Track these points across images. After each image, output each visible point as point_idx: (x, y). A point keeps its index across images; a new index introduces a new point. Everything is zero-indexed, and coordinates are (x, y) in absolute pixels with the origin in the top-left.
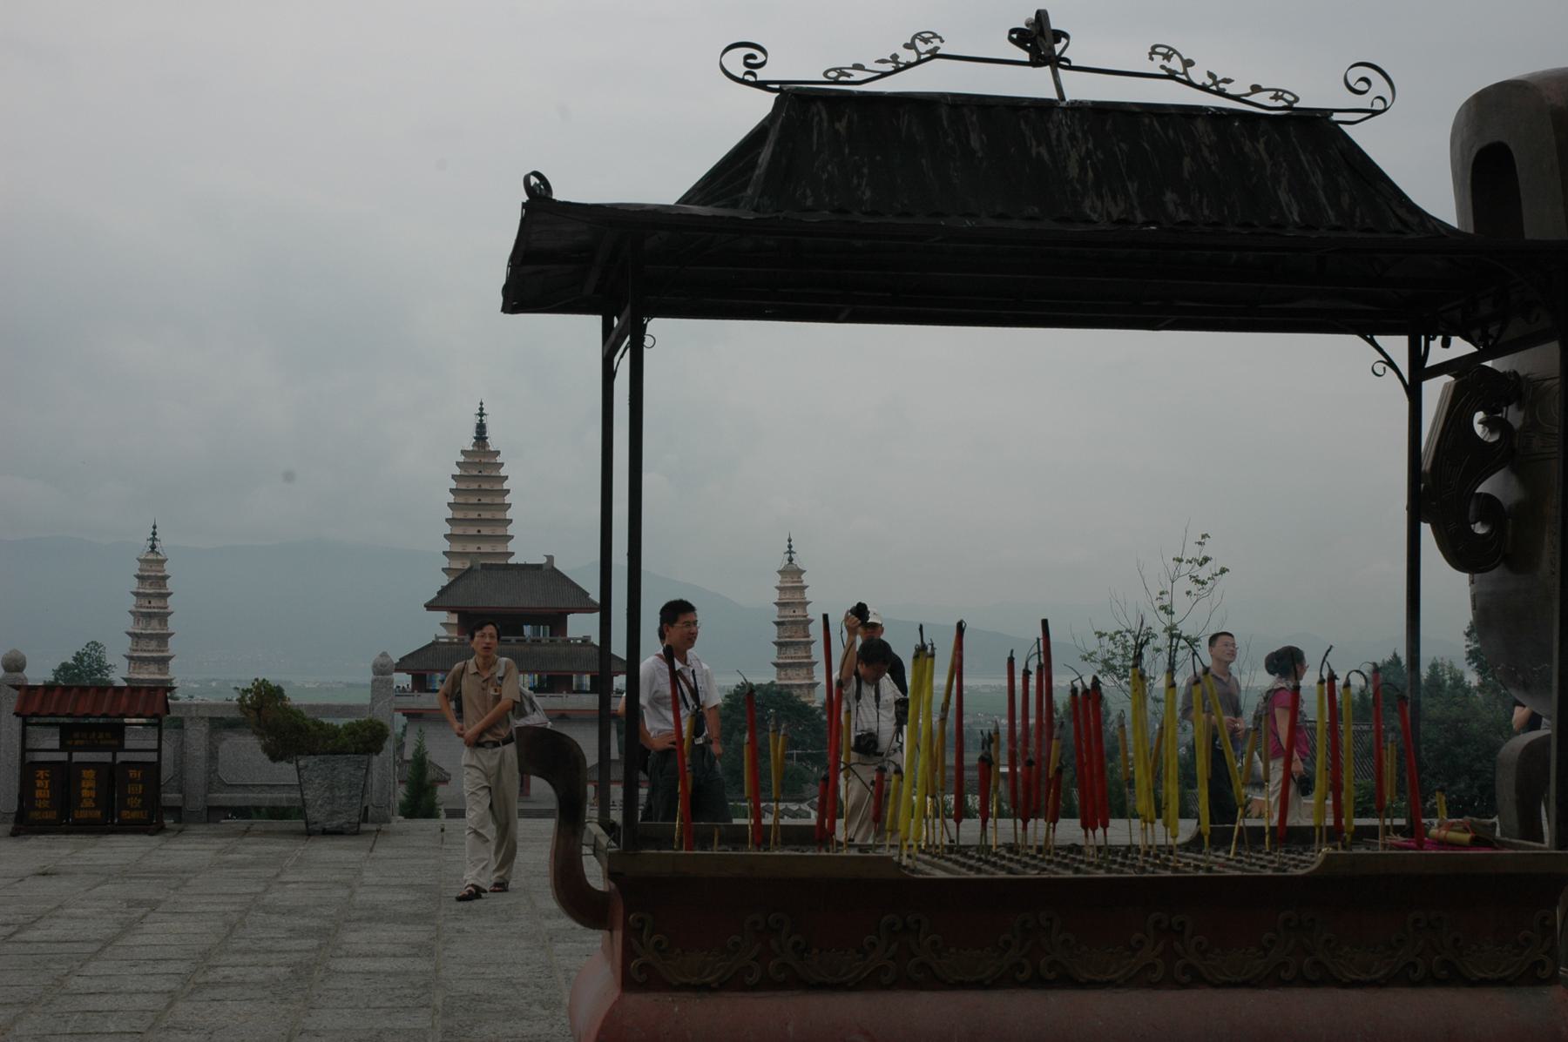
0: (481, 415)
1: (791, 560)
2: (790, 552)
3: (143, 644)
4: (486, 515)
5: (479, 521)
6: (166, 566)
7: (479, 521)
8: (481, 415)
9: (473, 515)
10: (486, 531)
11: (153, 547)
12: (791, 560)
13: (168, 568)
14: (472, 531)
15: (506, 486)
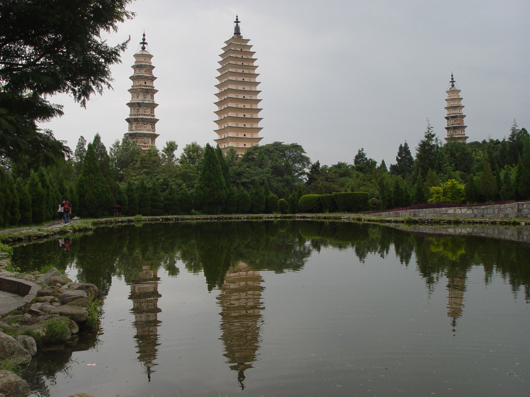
0: (237, 22)
1: (453, 86)
2: (453, 82)
3: (141, 111)
4: (246, 71)
5: (243, 74)
6: (152, 60)
7: (243, 74)
8: (237, 22)
9: (240, 71)
10: (247, 79)
11: (143, 48)
12: (453, 86)
13: (153, 62)
14: (240, 79)
15: (254, 57)
